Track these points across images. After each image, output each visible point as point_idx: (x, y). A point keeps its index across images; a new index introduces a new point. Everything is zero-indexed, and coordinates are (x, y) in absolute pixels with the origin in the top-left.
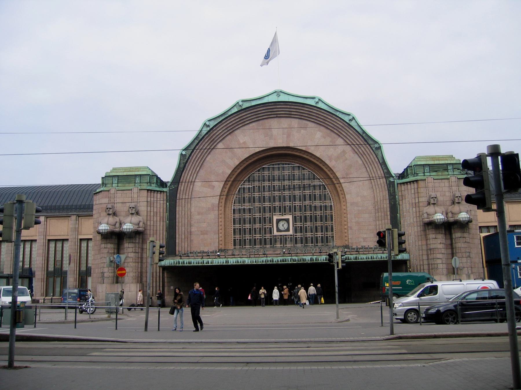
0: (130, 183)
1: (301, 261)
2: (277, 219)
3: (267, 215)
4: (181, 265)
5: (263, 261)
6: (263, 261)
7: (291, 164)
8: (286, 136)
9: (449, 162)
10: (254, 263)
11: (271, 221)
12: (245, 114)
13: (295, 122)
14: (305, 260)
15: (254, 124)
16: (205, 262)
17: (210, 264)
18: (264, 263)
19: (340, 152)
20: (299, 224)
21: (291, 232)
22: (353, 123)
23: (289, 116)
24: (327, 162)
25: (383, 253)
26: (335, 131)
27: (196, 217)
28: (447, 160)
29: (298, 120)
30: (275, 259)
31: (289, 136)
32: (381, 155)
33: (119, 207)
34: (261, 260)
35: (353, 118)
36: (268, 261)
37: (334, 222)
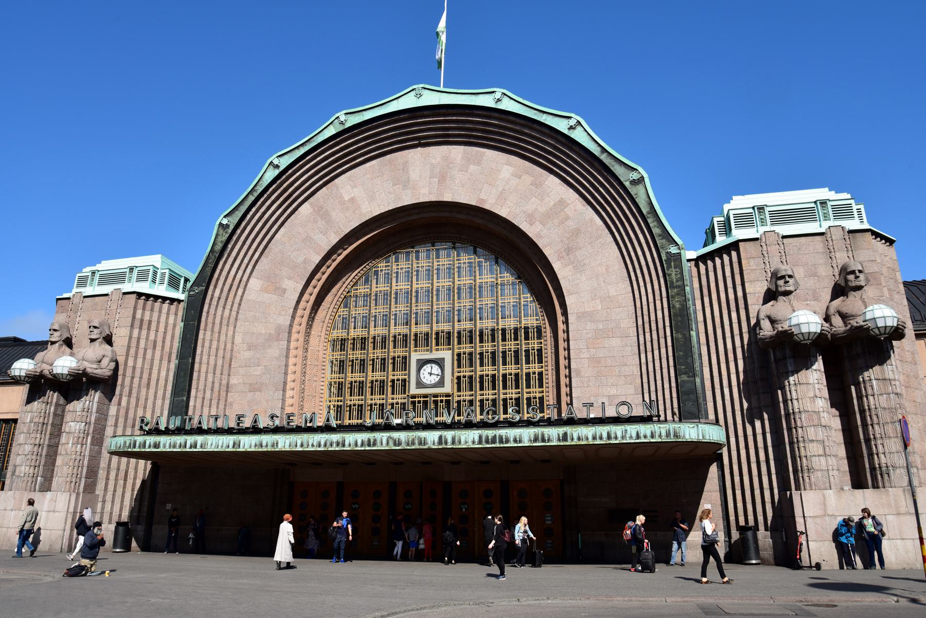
1: (413, 443)
2: (418, 360)
8: (436, 180)
13: (457, 152)
16: (188, 445)
17: (198, 449)
18: (322, 449)
19: (552, 203)
20: (466, 372)
21: (448, 388)
23: (445, 140)
24: (524, 227)
27: (243, 354)
29: (462, 147)
31: (443, 178)
35: (579, 123)
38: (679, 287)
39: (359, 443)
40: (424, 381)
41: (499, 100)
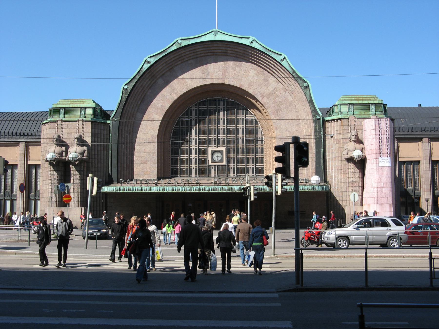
0: (75, 114)
2: (212, 151)
3: (203, 147)
4: (121, 191)
5: (196, 190)
6: (196, 190)
7: (226, 100)
8: (221, 73)
9: (372, 102)
10: (188, 191)
11: (206, 152)
12: (184, 51)
14: (234, 190)
15: (192, 61)
16: (143, 190)
17: (148, 191)
22: (284, 63)
24: (259, 99)
25: (305, 185)
26: (268, 69)
28: (370, 100)
30: (207, 188)
32: (309, 94)
33: (65, 138)
34: (194, 189)
35: (285, 58)
36: (200, 190)
37: (264, 154)
38: (318, 132)
39: (211, 189)
40: (214, 159)
41: (252, 42)
